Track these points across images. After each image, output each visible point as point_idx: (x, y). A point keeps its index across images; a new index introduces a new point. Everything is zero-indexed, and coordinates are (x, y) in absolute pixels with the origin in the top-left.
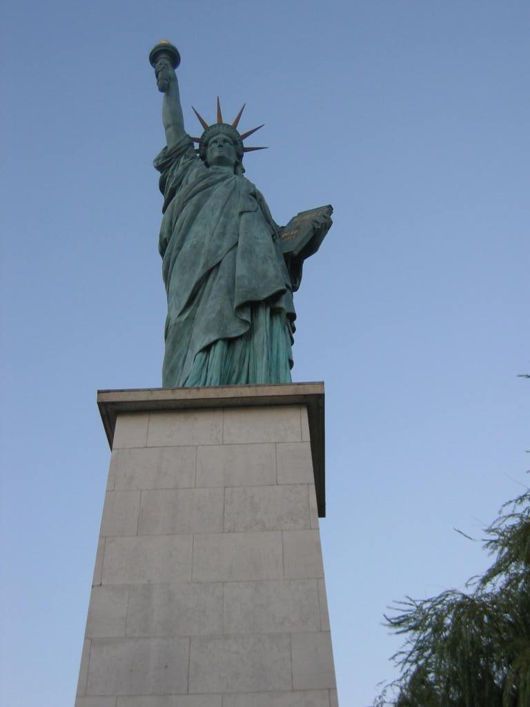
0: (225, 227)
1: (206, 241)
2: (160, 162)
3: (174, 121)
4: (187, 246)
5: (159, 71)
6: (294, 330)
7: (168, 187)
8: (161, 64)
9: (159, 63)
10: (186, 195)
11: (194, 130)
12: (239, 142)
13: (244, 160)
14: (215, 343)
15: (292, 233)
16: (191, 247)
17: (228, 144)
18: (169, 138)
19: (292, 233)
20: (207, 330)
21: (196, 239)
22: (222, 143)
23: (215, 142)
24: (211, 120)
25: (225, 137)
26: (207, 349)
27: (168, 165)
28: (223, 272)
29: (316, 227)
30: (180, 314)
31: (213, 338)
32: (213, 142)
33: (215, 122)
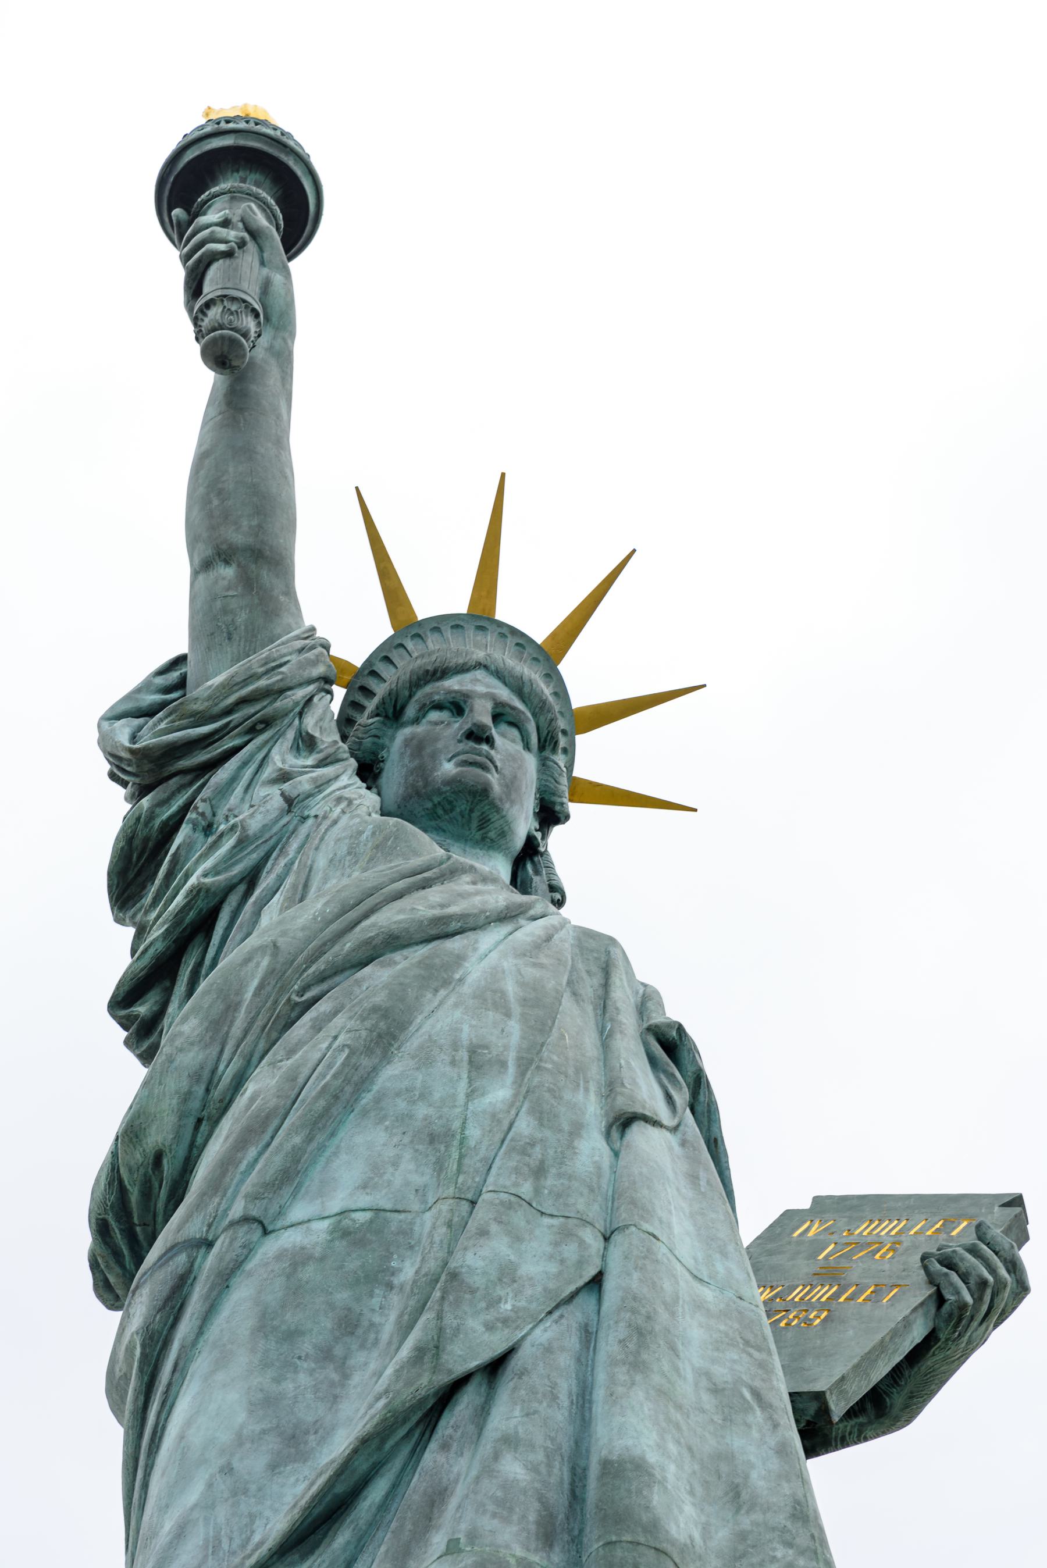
2: (155, 734)
4: (306, 1224)
7: (187, 876)
8: (226, 223)
9: (212, 216)
10: (320, 952)
11: (341, 615)
12: (562, 742)
13: (557, 831)
15: (796, 1295)
16: (344, 1232)
17: (514, 732)
18: (211, 622)
19: (796, 1295)
21: (365, 1200)
22: (487, 720)
23: (457, 706)
24: (440, 591)
25: (504, 694)
33: (456, 600)
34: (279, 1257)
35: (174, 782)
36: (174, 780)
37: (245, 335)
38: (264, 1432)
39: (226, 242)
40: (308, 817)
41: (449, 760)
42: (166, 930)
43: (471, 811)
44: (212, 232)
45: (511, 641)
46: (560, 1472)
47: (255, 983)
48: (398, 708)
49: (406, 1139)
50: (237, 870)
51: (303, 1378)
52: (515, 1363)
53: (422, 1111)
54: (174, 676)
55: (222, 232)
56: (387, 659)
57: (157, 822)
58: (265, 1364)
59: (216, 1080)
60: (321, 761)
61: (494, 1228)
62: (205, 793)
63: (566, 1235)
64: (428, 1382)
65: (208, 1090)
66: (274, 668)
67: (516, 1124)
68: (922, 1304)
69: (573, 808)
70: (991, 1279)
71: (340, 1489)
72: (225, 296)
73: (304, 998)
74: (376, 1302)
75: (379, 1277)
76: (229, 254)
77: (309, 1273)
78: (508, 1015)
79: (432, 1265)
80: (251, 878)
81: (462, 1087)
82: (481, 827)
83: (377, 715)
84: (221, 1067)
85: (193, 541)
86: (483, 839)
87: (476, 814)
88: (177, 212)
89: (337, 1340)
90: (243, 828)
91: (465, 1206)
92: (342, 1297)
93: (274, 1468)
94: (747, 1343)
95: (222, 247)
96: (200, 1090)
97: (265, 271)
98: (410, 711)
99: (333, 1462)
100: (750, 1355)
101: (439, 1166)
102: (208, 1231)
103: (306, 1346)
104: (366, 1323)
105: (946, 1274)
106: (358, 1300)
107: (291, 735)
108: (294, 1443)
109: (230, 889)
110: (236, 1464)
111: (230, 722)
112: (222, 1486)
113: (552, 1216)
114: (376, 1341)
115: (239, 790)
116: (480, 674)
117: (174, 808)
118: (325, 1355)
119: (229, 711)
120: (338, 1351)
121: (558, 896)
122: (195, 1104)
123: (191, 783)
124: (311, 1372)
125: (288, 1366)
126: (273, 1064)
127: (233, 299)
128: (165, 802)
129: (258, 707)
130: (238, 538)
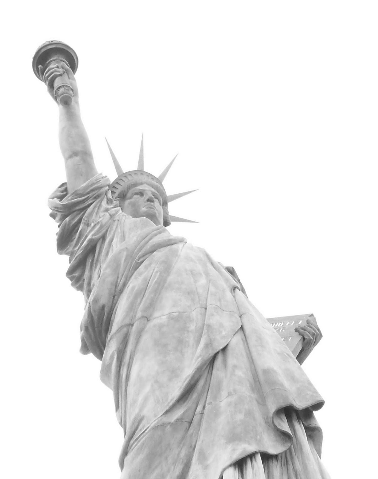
3: (78, 152)
7: (86, 237)
8: (57, 67)
9: (52, 66)
14: (252, 456)
20: (233, 438)
21: (175, 310)
24: (129, 165)
26: (240, 464)
27: (78, 208)
28: (236, 358)
29: (306, 337)
30: (167, 412)
31: (251, 448)
35: (75, 213)
36: (75, 213)
37: (71, 95)
39: (59, 72)
40: (115, 220)
41: (143, 207)
42: (83, 252)
44: (55, 70)
45: (150, 177)
47: (124, 259)
48: (124, 195)
50: (100, 235)
52: (229, 347)
54: (63, 188)
56: (117, 183)
57: (71, 225)
59: (118, 285)
60: (115, 206)
61: (215, 314)
62: (86, 215)
64: (212, 353)
65: (116, 288)
66: (98, 182)
67: (210, 288)
68: (300, 340)
69: (171, 222)
70: (315, 333)
71: (192, 383)
72: (64, 85)
73: (139, 261)
75: (184, 329)
76: (61, 75)
77: (165, 329)
79: (200, 324)
80: (104, 237)
81: (192, 280)
83: (118, 198)
84: (119, 281)
85: (64, 152)
88: (40, 66)
90: (101, 223)
91: (204, 309)
93: (170, 380)
96: (114, 287)
97: (70, 80)
98: (129, 195)
99: (189, 375)
101: (193, 300)
102: (131, 321)
105: (305, 332)
107: (105, 200)
108: (174, 373)
109: (98, 240)
111: (89, 197)
113: (226, 311)
114: (189, 345)
115: (95, 214)
116: (145, 185)
117: (76, 220)
119: (88, 193)
122: (113, 291)
123: (79, 214)
126: (136, 278)
127: (66, 86)
128: (73, 219)
129: (96, 192)
130: (79, 148)
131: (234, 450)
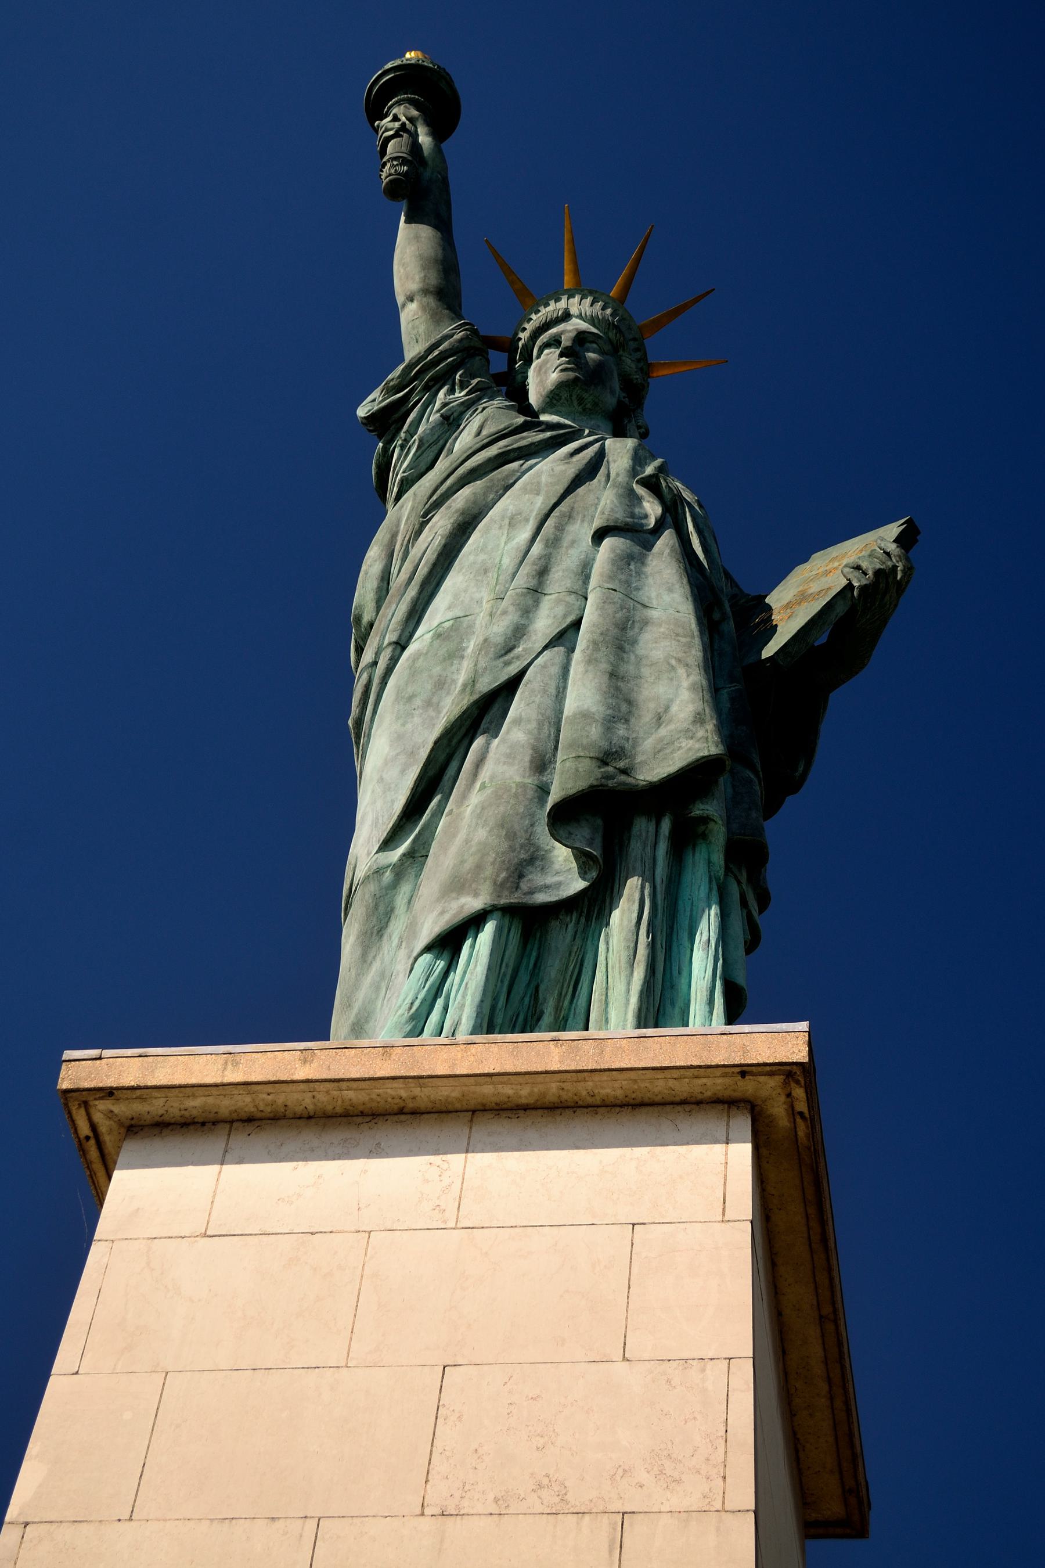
0: (543, 572)
1: (481, 619)
5: (388, 139)
6: (764, 900)
16: (438, 636)
21: (450, 615)
23: (555, 342)
25: (584, 326)
26: (449, 943)
31: (473, 904)
32: (547, 345)
34: (407, 660)
38: (398, 754)
43: (571, 396)
46: (547, 730)
47: (404, 519)
49: (472, 576)
51: (417, 720)
53: (482, 557)
55: (391, 125)
58: (398, 718)
63: (558, 601)
71: (431, 773)
74: (454, 668)
77: (420, 663)
78: (538, 494)
79: (481, 639)
81: (504, 538)
82: (580, 404)
84: (394, 570)
86: (584, 410)
87: (574, 397)
89: (433, 694)
92: (437, 670)
94: (677, 635)
95: (391, 133)
100: (678, 641)
103: (418, 702)
104: (449, 681)
106: (444, 670)
110: (384, 776)
112: (379, 790)
118: (428, 703)
120: (435, 700)
121: (643, 430)
124: (421, 715)
125: (410, 715)
131: (443, 913)
